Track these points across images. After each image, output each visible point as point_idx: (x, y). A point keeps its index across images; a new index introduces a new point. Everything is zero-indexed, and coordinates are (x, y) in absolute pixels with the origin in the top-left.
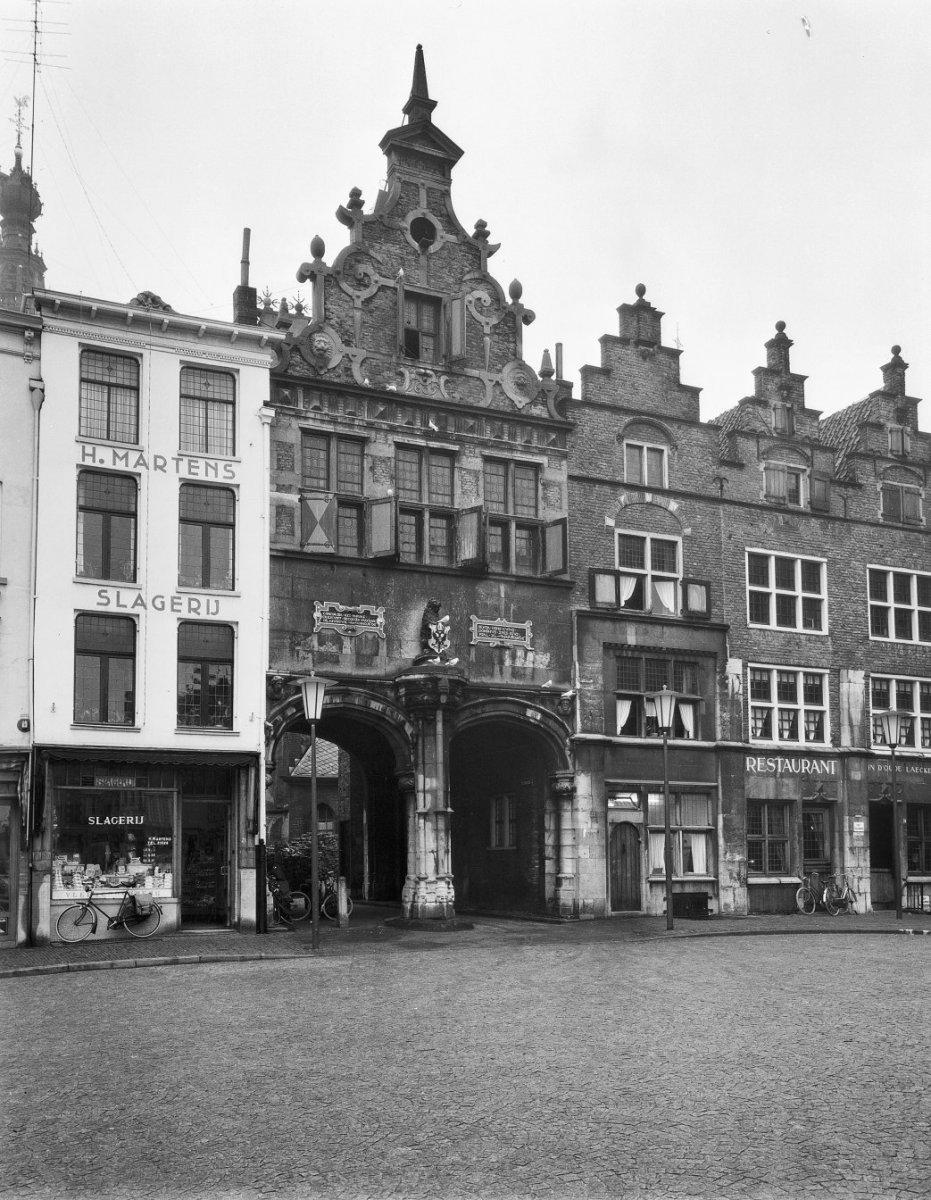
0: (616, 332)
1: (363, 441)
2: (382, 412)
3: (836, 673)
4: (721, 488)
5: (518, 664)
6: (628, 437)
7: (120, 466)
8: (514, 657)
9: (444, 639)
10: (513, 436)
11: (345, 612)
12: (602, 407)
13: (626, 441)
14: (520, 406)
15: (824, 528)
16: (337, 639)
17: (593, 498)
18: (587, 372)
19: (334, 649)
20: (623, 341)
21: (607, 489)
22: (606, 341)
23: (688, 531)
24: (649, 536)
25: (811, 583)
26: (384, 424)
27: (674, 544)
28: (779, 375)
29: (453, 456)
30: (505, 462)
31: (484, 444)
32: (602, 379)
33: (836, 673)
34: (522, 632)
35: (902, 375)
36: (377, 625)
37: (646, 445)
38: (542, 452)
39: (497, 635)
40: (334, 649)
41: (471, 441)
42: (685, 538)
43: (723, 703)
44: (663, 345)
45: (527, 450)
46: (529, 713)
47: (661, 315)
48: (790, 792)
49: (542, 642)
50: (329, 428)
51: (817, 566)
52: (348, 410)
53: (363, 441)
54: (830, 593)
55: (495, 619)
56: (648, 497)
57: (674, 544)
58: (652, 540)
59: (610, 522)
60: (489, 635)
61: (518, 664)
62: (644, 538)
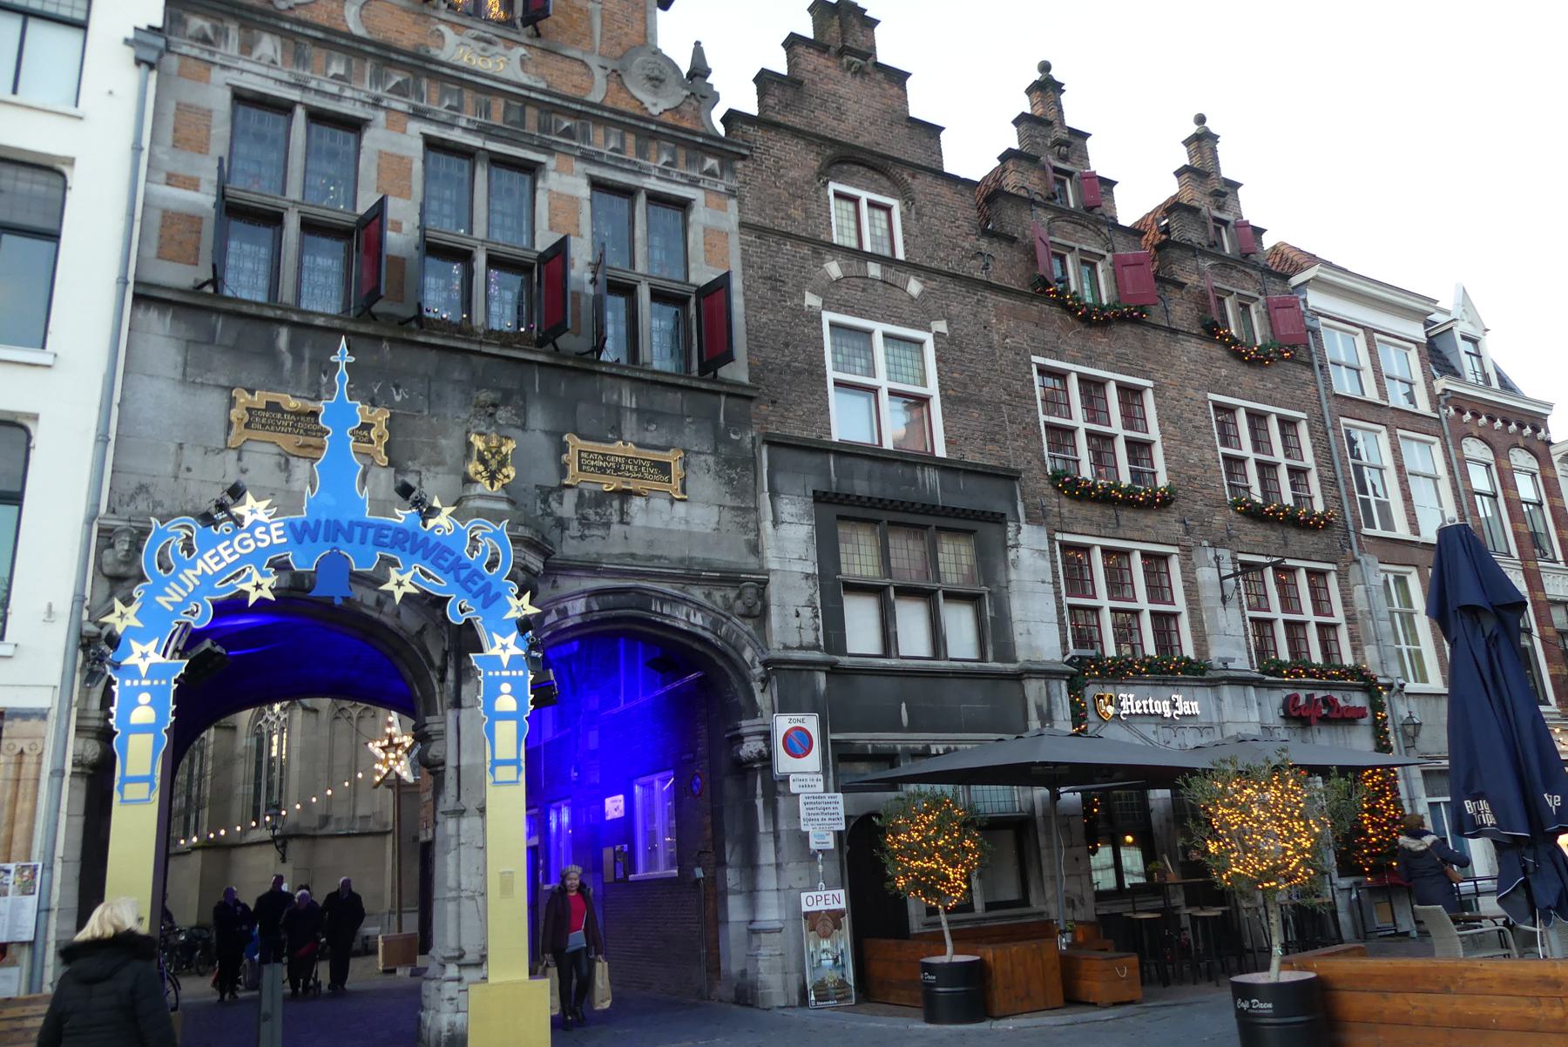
0: (809, 33)
1: (355, 126)
2: (398, 84)
3: (1187, 552)
4: (986, 268)
6: (835, 179)
9: (502, 464)
10: (641, 153)
11: (297, 414)
12: (796, 133)
13: (833, 186)
14: (655, 111)
15: (1143, 340)
17: (781, 260)
18: (765, 80)
20: (817, 45)
22: (793, 43)
23: (941, 326)
24: (879, 328)
25: (1132, 417)
26: (400, 105)
27: (921, 343)
28: (1048, 137)
29: (532, 169)
30: (628, 193)
31: (587, 158)
32: (790, 93)
34: (664, 468)
35: (1214, 151)
36: (371, 442)
37: (865, 196)
38: (693, 183)
39: (617, 470)
41: (568, 152)
42: (938, 335)
44: (881, 59)
45: (664, 175)
47: (876, 22)
50: (294, 95)
51: (1138, 391)
52: (331, 73)
53: (355, 126)
54: (1162, 432)
55: (612, 441)
56: (874, 270)
57: (921, 343)
58: (886, 336)
59: (812, 300)
60: (602, 470)
62: (869, 333)
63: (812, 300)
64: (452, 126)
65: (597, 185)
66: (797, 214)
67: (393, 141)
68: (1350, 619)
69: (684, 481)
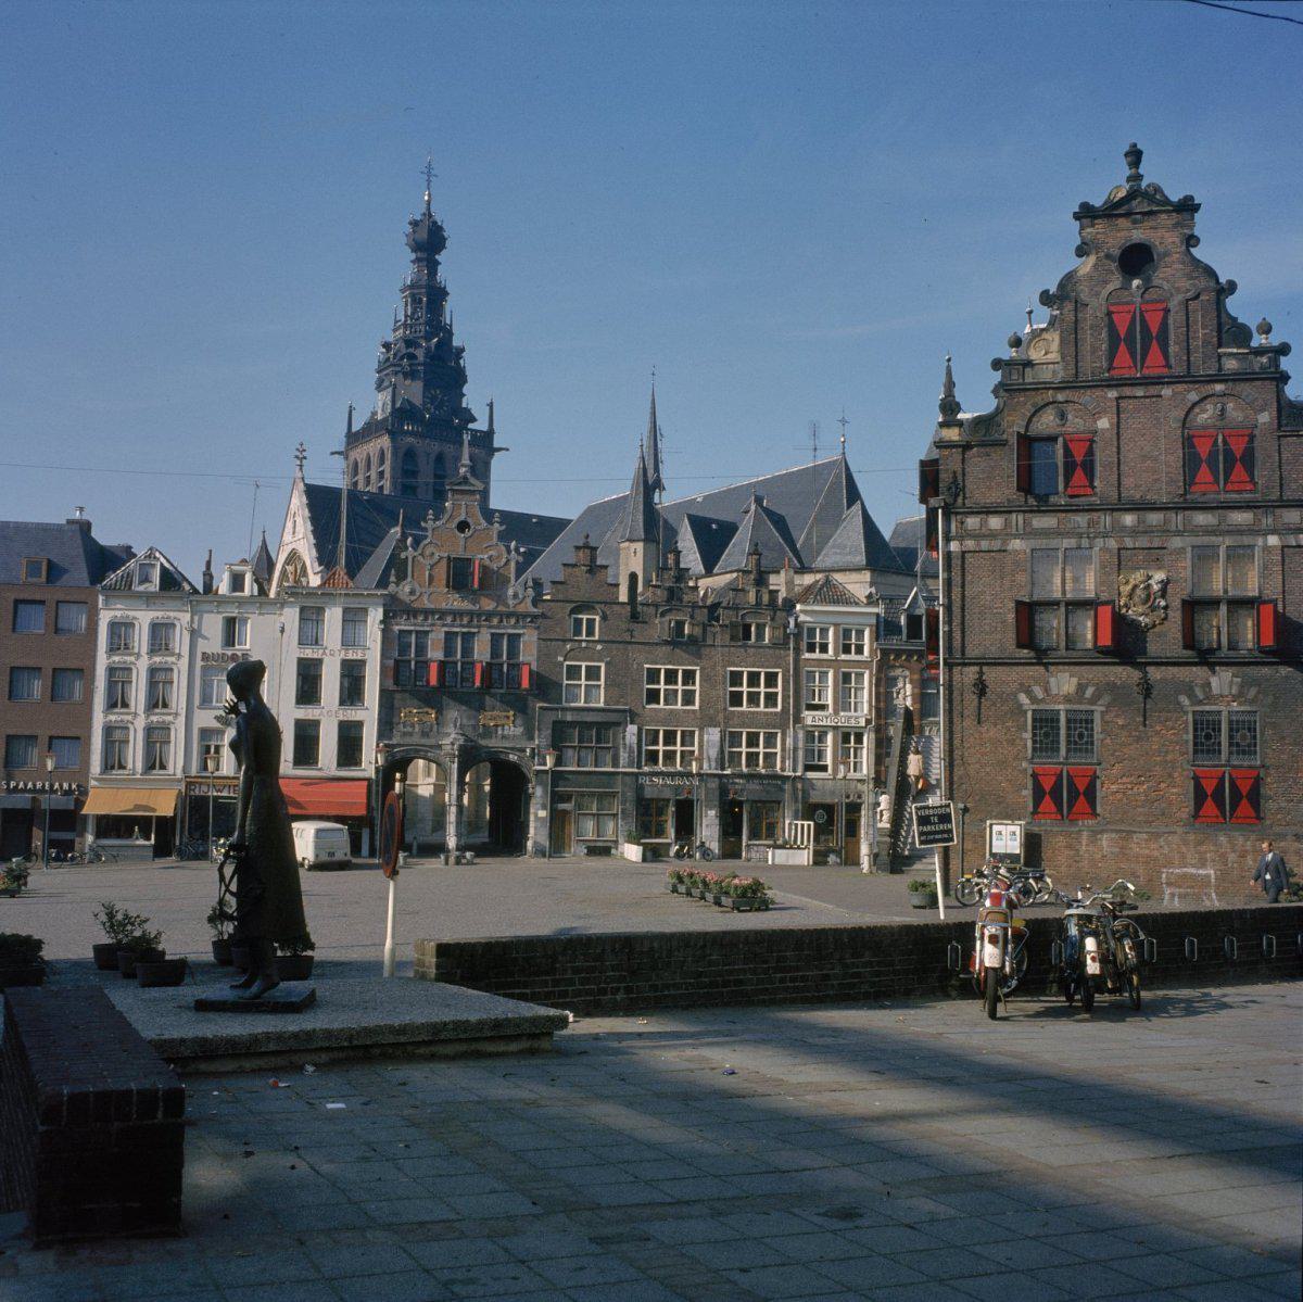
1: (427, 633)
3: (701, 730)
5: (506, 732)
7: (315, 656)
8: (503, 730)
16: (413, 726)
19: (410, 730)
21: (560, 643)
24: (584, 664)
33: (701, 730)
34: (508, 717)
38: (524, 627)
40: (410, 730)
41: (484, 626)
42: (607, 664)
43: (625, 748)
45: (514, 627)
46: (511, 756)
48: (667, 794)
49: (518, 721)
50: (412, 628)
54: (701, 685)
59: (560, 659)
61: (506, 732)
63: (560, 659)
64: (453, 626)
65: (492, 634)
66: (558, 630)
67: (436, 637)
68: (783, 750)
69: (513, 721)
